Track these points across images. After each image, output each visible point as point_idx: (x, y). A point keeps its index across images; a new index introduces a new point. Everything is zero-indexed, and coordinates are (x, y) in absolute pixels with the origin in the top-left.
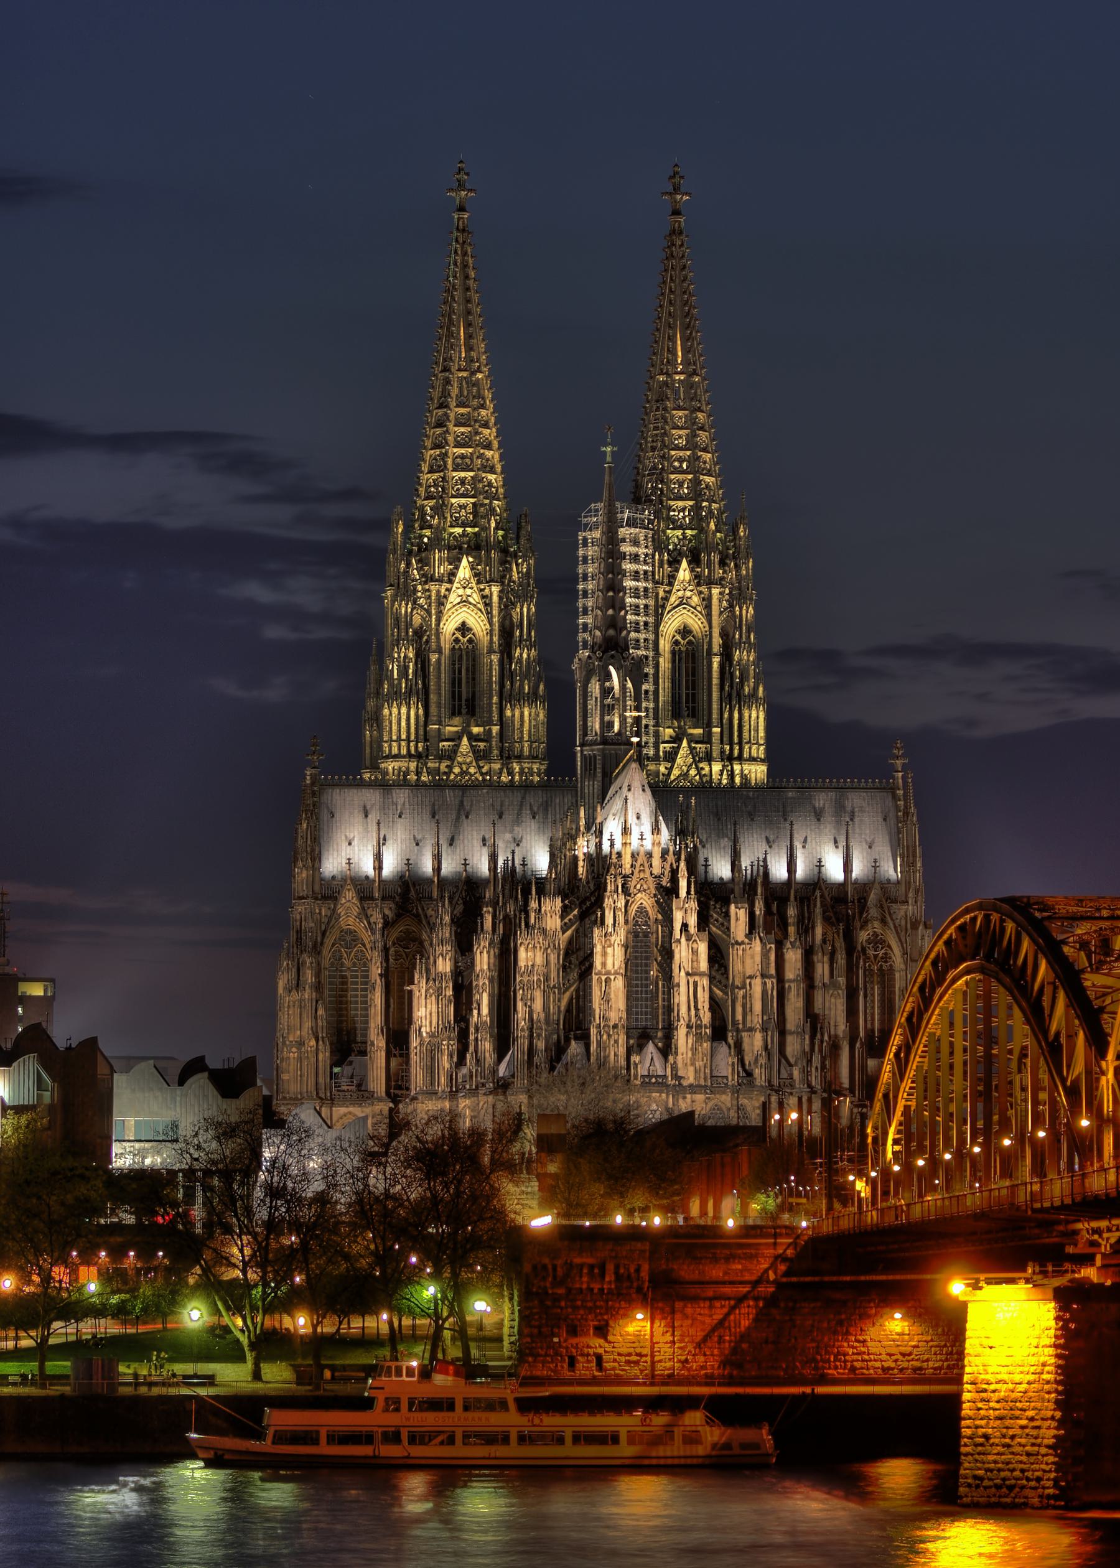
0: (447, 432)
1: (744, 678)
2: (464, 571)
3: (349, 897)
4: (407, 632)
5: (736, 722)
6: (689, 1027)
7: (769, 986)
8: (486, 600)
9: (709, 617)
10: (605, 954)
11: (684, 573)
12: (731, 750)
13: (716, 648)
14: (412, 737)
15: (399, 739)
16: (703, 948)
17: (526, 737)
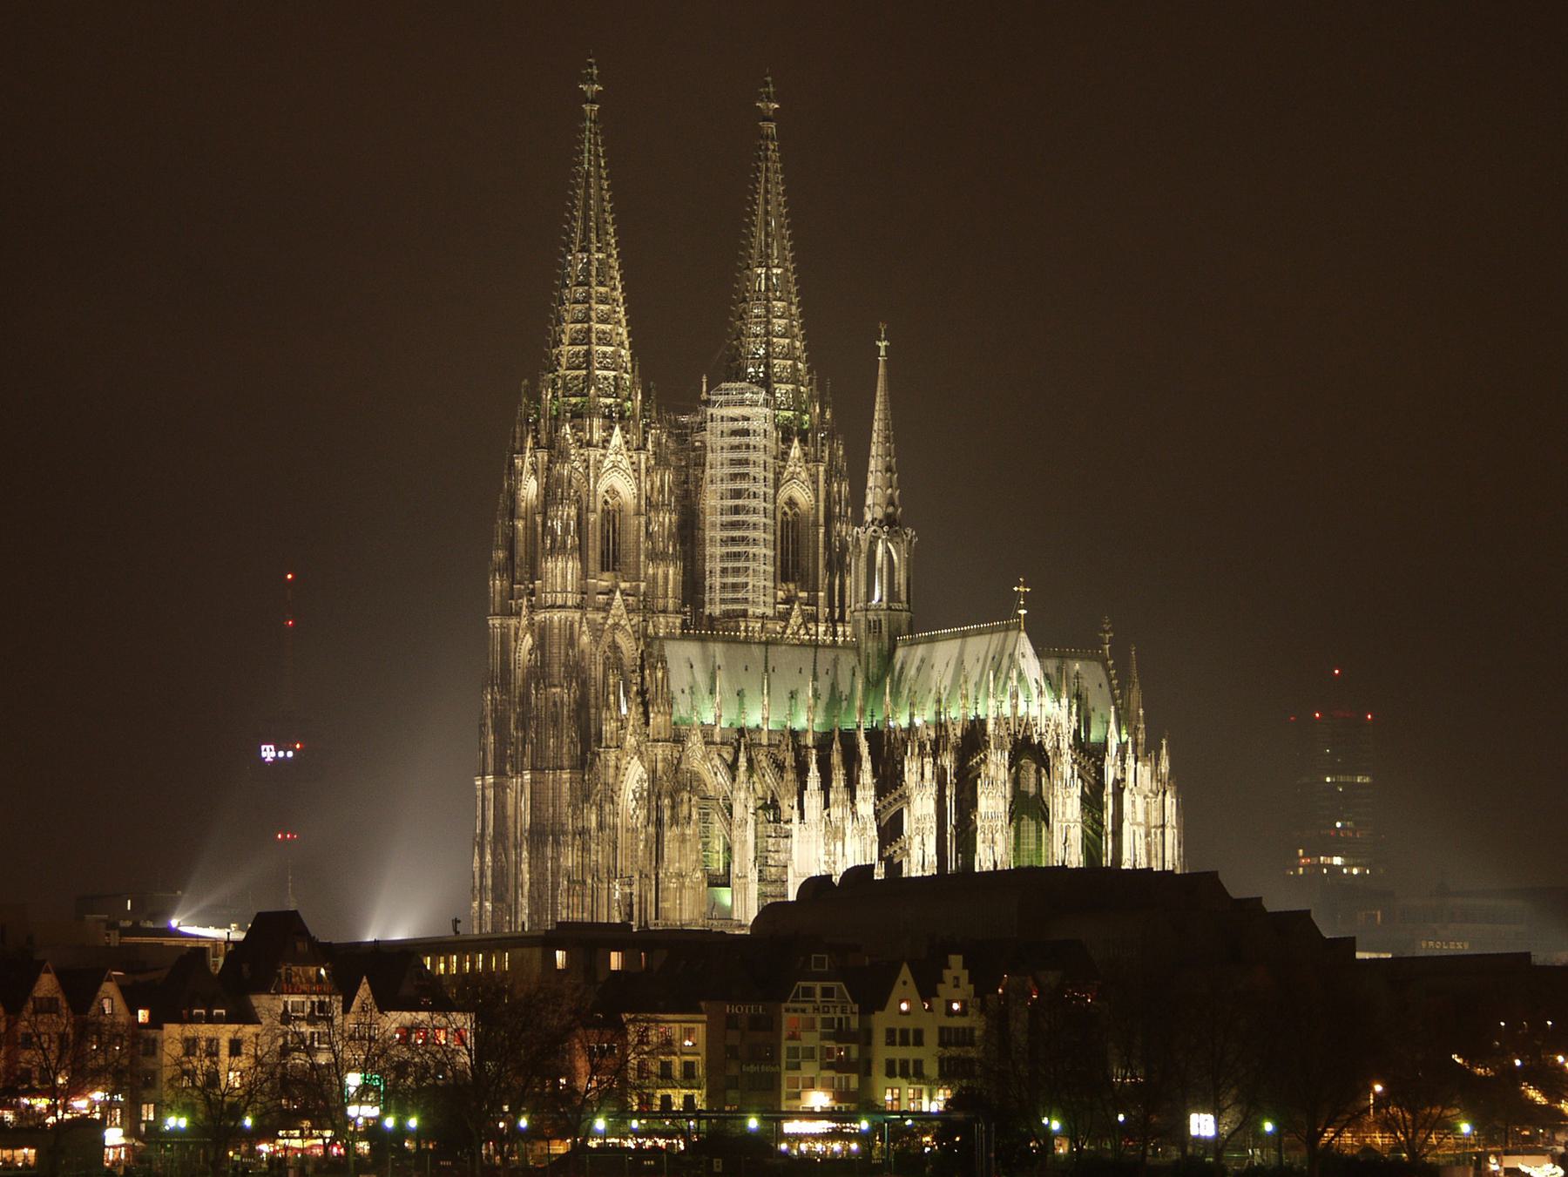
0: (590, 308)
2: (617, 438)
3: (695, 743)
9: (816, 491)
12: (832, 612)
13: (822, 520)
17: (670, 593)
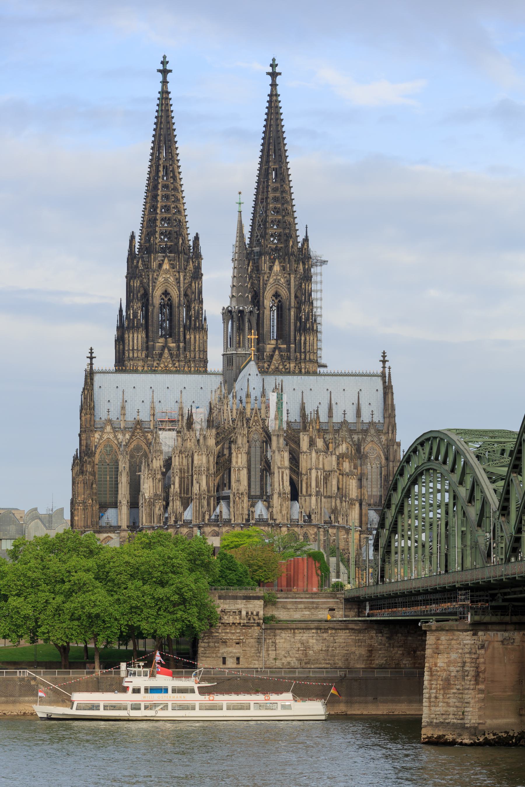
1: (307, 319)
4: (138, 296)
5: (302, 342)
6: (280, 494)
7: (319, 473)
8: (178, 281)
10: (237, 457)
11: (277, 268)
14: (140, 348)
15: (133, 349)
16: (286, 455)
